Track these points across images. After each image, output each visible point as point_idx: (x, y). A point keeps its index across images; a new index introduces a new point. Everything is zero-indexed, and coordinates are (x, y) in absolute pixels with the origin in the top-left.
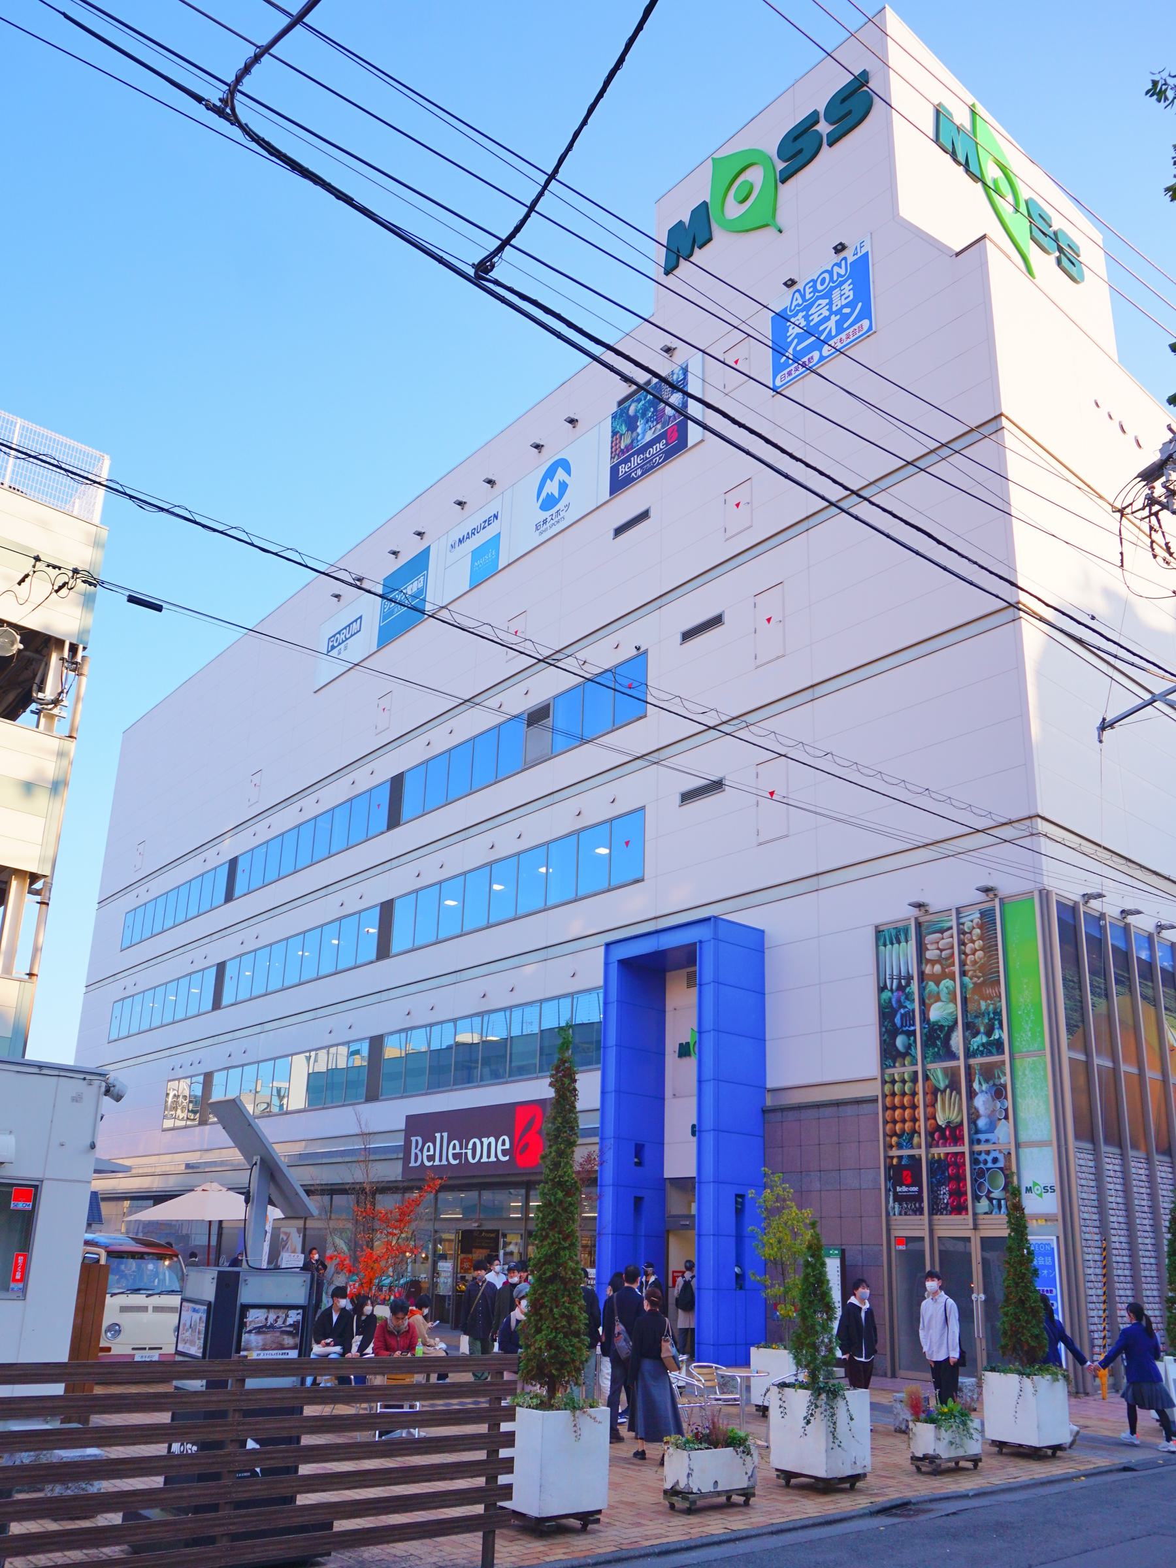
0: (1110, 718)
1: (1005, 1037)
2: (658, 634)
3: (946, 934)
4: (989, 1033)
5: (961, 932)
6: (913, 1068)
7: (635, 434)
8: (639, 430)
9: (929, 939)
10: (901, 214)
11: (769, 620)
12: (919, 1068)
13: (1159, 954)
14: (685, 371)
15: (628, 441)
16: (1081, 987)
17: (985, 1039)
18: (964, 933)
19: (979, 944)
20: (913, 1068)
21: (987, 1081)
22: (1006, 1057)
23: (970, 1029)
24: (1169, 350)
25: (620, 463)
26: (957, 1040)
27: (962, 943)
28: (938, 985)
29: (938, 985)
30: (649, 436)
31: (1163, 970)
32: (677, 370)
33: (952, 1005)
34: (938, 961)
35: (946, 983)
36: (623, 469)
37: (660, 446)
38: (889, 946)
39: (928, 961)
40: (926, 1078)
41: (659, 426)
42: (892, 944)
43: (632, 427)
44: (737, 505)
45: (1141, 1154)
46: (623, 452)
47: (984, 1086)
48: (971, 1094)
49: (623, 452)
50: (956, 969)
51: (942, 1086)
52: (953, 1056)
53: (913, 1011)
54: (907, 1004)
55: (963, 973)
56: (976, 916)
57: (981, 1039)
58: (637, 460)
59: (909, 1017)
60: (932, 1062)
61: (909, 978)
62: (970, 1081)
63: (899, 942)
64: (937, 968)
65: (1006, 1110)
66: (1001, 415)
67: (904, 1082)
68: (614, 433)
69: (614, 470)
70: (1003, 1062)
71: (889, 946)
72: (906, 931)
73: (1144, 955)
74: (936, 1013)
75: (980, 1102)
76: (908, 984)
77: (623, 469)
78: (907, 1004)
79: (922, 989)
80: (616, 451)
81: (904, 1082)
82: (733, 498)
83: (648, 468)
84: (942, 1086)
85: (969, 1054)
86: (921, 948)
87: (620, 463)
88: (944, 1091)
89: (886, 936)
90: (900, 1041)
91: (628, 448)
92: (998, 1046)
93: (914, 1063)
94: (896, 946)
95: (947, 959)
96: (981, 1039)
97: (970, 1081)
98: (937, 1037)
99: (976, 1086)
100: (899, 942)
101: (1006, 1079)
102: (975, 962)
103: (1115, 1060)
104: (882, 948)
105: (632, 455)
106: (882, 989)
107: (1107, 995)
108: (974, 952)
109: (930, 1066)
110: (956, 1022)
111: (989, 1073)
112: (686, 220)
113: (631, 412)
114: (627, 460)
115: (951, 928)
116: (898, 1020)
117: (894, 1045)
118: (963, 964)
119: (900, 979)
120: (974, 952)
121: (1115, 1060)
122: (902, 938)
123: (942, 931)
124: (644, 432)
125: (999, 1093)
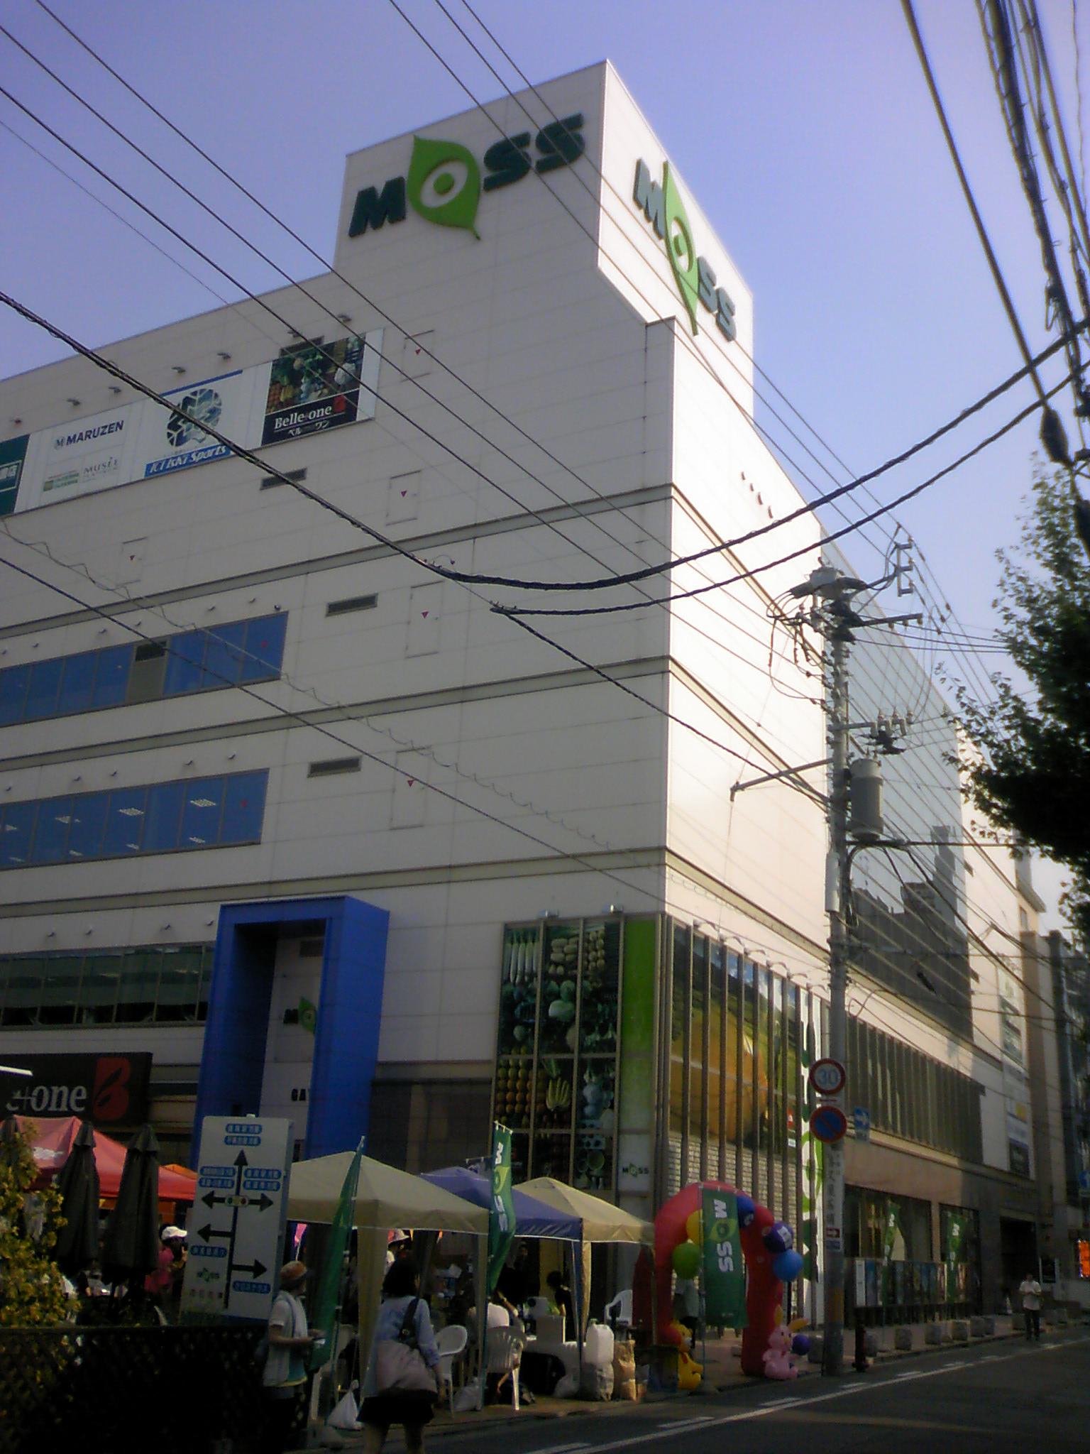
0: (741, 783)
1: (618, 1038)
2: (302, 601)
3: (572, 940)
4: (603, 1031)
5: (587, 941)
6: (529, 1057)
7: (297, 391)
8: (303, 388)
9: (555, 942)
10: (604, 265)
11: (425, 614)
12: (535, 1058)
13: (744, 972)
14: (362, 343)
15: (289, 396)
16: (686, 1001)
17: (598, 1038)
18: (589, 941)
19: (601, 953)
20: (529, 1057)
21: (597, 1073)
22: (617, 1055)
23: (587, 1027)
24: (1047, 909)
25: (278, 415)
26: (573, 1036)
27: (586, 951)
28: (559, 985)
29: (559, 985)
30: (313, 399)
31: (746, 986)
32: (353, 339)
33: (570, 1006)
34: (563, 963)
35: (567, 984)
36: (279, 423)
37: (326, 411)
38: (516, 945)
39: (552, 963)
40: (540, 1066)
41: (326, 391)
42: (519, 942)
43: (295, 381)
44: (404, 493)
45: (717, 1142)
46: (281, 405)
47: (594, 1079)
48: (582, 1084)
49: (281, 405)
50: (579, 973)
51: (554, 1074)
52: (568, 1050)
53: (534, 1006)
54: (530, 1000)
55: (585, 977)
56: (601, 928)
57: (595, 1037)
58: (296, 418)
59: (530, 1010)
60: (547, 1053)
61: (532, 975)
62: (581, 1074)
63: (526, 942)
64: (560, 970)
65: (612, 1102)
66: (672, 485)
67: (518, 1068)
68: (274, 382)
69: (270, 421)
70: (614, 1060)
71: (516, 945)
72: (534, 933)
73: (733, 973)
74: (554, 1009)
75: (588, 1092)
76: (531, 980)
77: (279, 423)
78: (530, 1000)
79: (544, 987)
80: (273, 402)
81: (518, 1068)
82: (401, 484)
83: (309, 429)
84: (554, 1074)
85: (583, 1049)
86: (547, 950)
87: (278, 415)
88: (555, 1080)
89: (515, 934)
90: (517, 1031)
91: (288, 402)
92: (611, 1045)
93: (530, 1051)
94: (522, 945)
95: (571, 962)
96: (595, 1037)
97: (581, 1074)
98: (554, 1031)
99: (586, 1077)
100: (526, 942)
101: (614, 1074)
102: (596, 969)
103: (704, 1063)
104: (509, 945)
105: (293, 411)
106: (505, 981)
107: (704, 1007)
108: (596, 959)
109: (545, 1056)
110: (573, 1019)
111: (600, 1067)
112: (380, 188)
113: (297, 364)
114: (286, 415)
115: (577, 935)
116: (517, 1011)
117: (512, 1034)
118: (585, 969)
119: (523, 974)
120: (596, 959)
121: (704, 1063)
122: (530, 938)
123: (568, 937)
124: (309, 392)
125: (607, 1085)
